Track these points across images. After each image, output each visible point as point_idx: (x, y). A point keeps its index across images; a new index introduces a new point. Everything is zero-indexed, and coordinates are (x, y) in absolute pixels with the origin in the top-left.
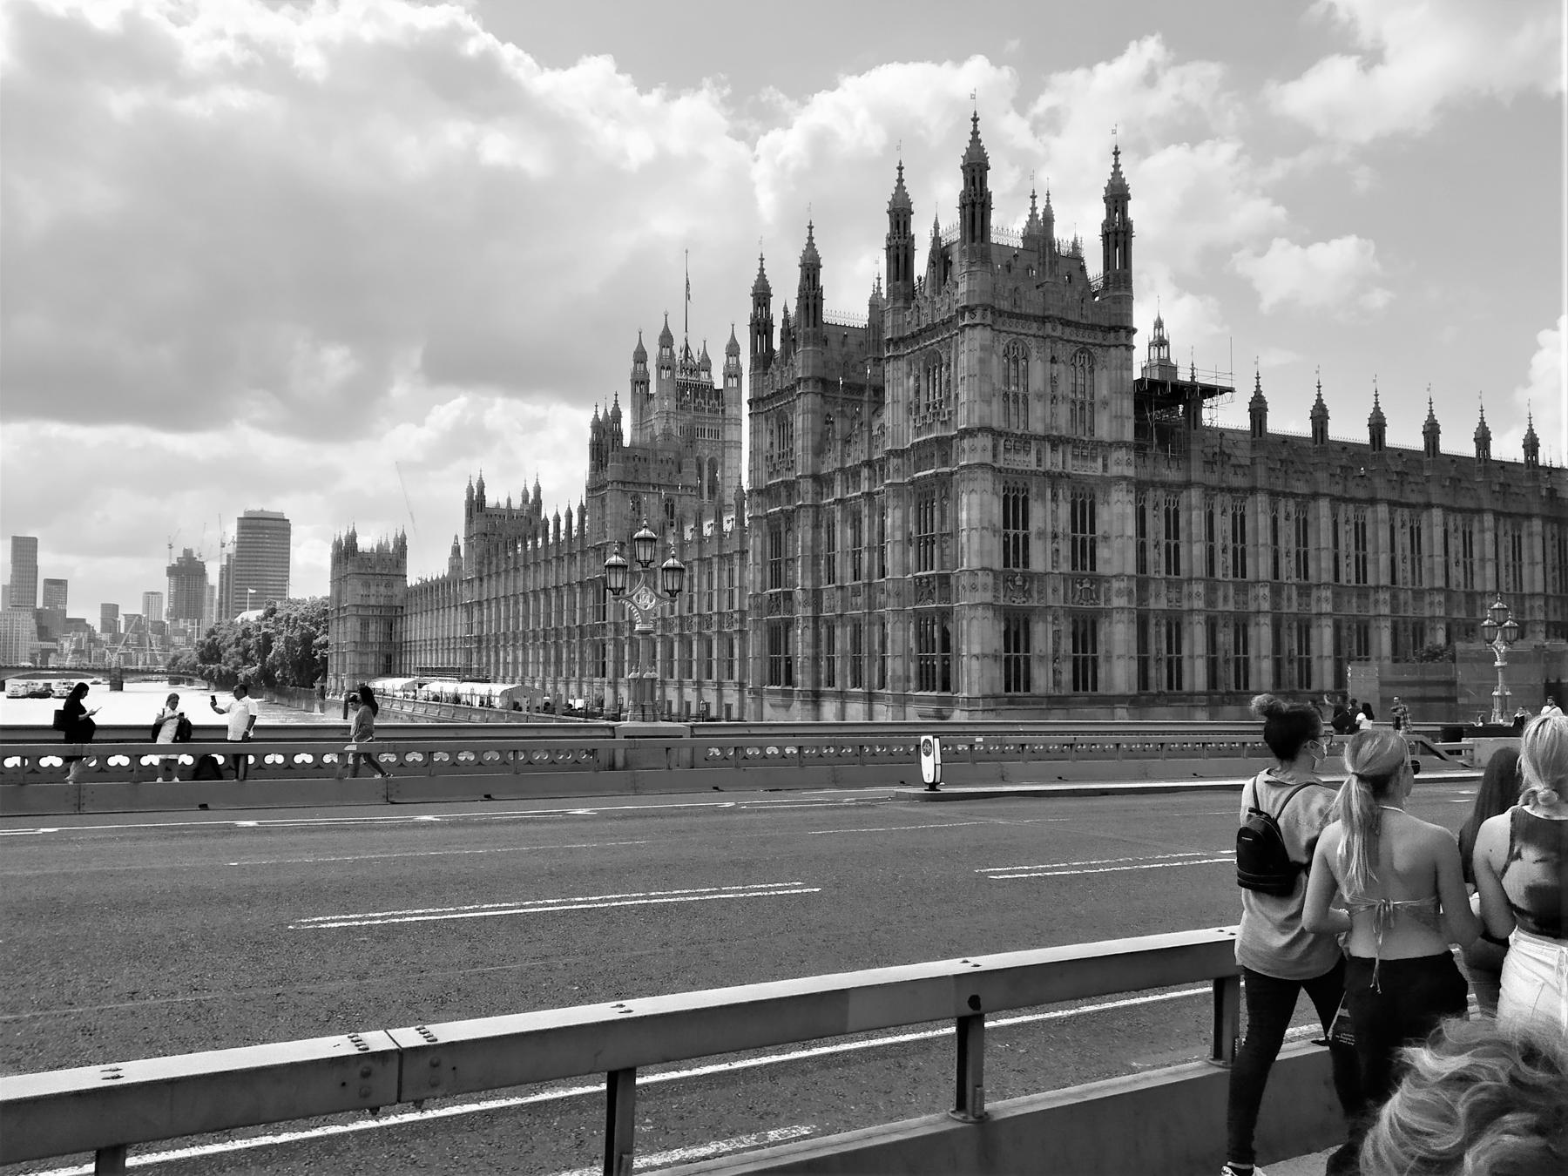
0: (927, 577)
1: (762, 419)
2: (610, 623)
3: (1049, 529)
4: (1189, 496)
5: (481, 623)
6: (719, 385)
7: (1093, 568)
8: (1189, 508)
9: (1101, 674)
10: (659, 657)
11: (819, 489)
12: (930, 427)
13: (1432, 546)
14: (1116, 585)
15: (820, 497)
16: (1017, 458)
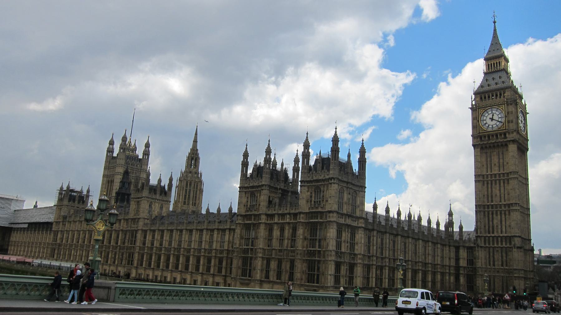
0: (313, 250)
1: (244, 193)
2: (138, 246)
3: (346, 240)
4: (373, 233)
5: (62, 239)
6: (141, 157)
7: (354, 251)
8: (373, 236)
9: (354, 281)
10: (162, 261)
11: (266, 219)
12: (317, 208)
13: (419, 250)
14: (359, 256)
15: (266, 220)
16: (340, 219)
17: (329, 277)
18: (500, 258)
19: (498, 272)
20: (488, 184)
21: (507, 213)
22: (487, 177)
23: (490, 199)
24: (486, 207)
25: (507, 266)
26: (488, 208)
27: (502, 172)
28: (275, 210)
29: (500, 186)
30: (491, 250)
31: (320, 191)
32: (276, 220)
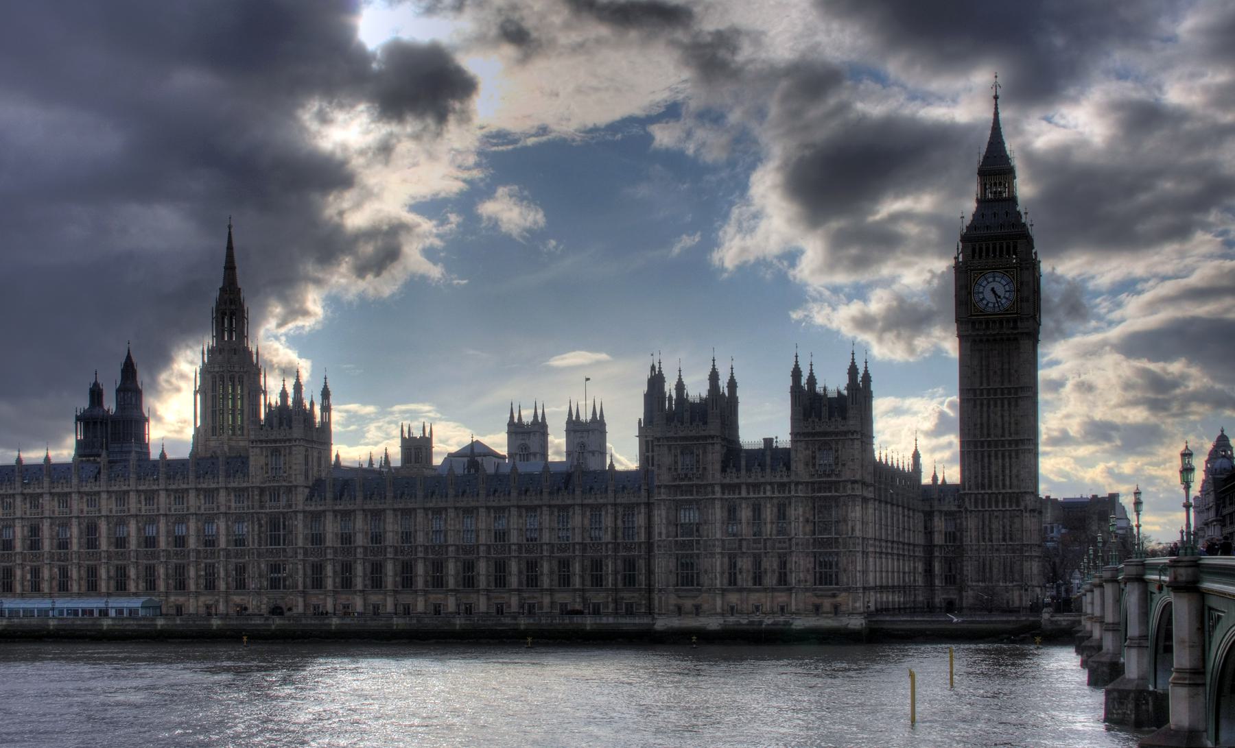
12: (829, 476)
17: (858, 574)
18: (1001, 528)
19: (997, 550)
20: (982, 405)
21: (1013, 454)
22: (982, 394)
23: (985, 431)
24: (979, 444)
25: (1011, 539)
26: (982, 446)
27: (1006, 385)
28: (738, 478)
29: (1003, 410)
30: (987, 515)
31: (831, 449)
32: (744, 494)
